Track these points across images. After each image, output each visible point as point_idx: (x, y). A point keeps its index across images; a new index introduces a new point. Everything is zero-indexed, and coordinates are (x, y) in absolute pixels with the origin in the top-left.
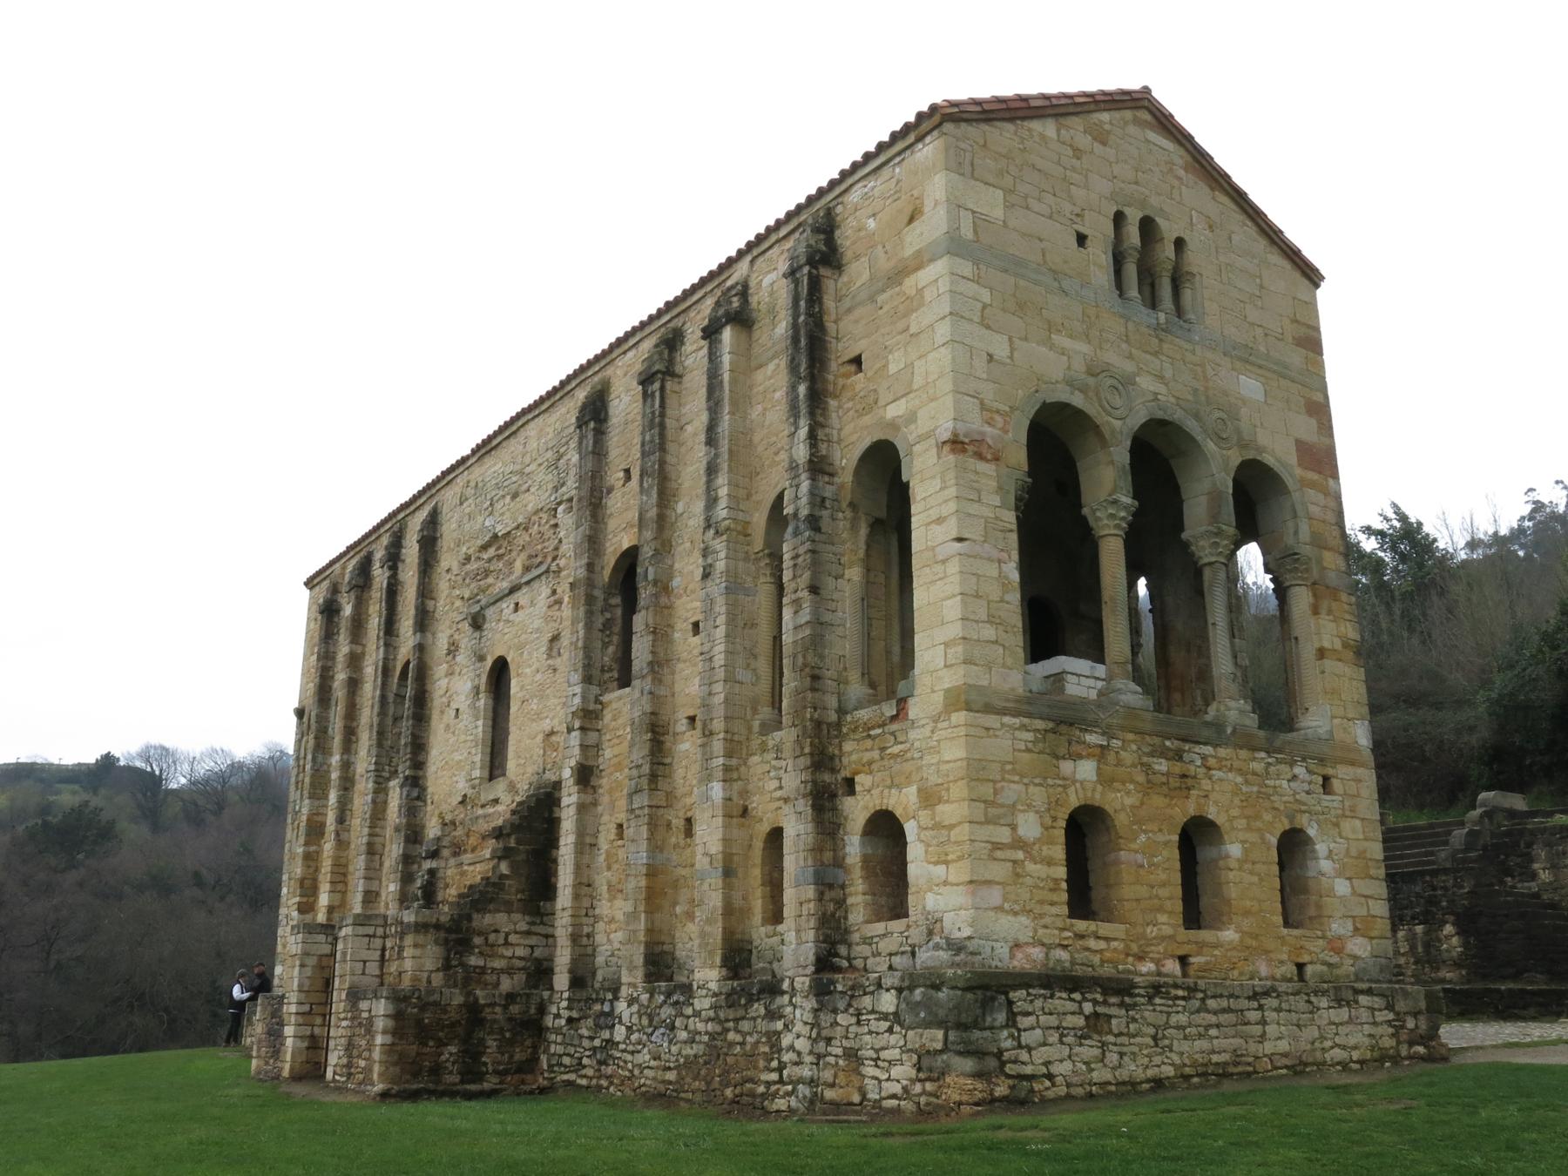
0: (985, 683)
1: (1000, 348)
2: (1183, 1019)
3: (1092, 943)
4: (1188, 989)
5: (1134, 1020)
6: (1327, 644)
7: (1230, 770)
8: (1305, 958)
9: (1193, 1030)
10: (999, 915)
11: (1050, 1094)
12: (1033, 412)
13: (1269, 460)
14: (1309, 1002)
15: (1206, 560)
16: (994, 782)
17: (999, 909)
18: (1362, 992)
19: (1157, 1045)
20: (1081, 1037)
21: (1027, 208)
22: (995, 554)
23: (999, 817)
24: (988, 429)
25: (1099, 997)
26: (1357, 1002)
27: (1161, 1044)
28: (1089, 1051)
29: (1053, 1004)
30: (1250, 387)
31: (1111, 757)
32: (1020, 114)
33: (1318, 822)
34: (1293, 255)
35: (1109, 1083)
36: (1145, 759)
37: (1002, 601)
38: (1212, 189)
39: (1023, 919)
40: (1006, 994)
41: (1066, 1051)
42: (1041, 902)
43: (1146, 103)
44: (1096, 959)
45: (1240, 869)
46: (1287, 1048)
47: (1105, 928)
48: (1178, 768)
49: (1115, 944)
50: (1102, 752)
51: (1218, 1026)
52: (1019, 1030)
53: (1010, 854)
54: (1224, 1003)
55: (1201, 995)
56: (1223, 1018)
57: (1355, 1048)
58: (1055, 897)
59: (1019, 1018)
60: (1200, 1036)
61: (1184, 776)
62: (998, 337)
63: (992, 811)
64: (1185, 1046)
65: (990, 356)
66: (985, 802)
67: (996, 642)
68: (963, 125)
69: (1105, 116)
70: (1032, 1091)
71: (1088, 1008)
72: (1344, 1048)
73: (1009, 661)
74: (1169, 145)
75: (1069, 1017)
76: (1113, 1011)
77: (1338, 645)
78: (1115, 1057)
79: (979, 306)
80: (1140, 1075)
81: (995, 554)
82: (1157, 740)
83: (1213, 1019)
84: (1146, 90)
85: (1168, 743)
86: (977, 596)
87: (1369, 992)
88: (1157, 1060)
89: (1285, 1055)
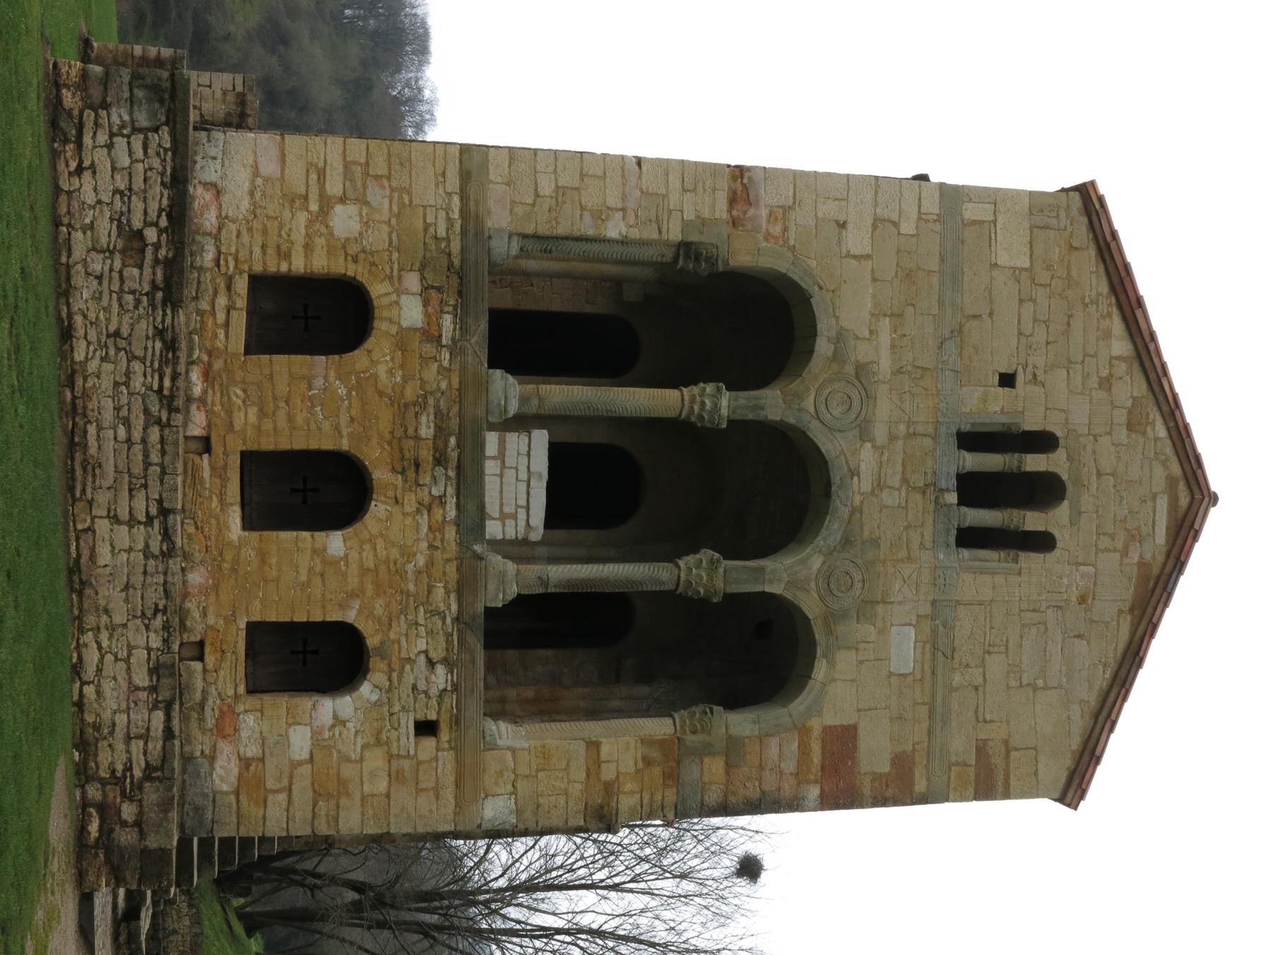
0: (492, 177)
1: (857, 240)
2: (137, 383)
3: (222, 301)
4: (172, 397)
5: (138, 303)
6: (605, 749)
7: (431, 547)
8: (210, 659)
9: (124, 400)
10: (249, 170)
11: (61, 166)
12: (796, 278)
13: (820, 670)
14: (156, 611)
16: (389, 178)
17: (256, 174)
18: (168, 718)
19: (108, 336)
20: (119, 221)
21: (1021, 301)
22: (631, 204)
23: (352, 181)
24: (764, 212)
25: (162, 252)
26: (156, 707)
27: (110, 342)
28: (106, 231)
29: (158, 189)
30: (904, 649)
31: (429, 349)
32: (1122, 297)
33: (378, 704)
35: (69, 256)
36: (431, 401)
37: (582, 208)
38: (1131, 610)
39: (245, 204)
40: (167, 124)
41: (106, 198)
42: (265, 232)
43: (1198, 496)
44: (204, 305)
45: (314, 551)
46: (101, 562)
47: (240, 321)
48: (426, 454)
49: (221, 334)
50: (430, 335)
51: (129, 440)
52: (128, 137)
53: (314, 190)
54: (155, 457)
55: (164, 418)
56: (138, 449)
59: (141, 136)
60: (117, 409)
61: (417, 465)
62: (867, 241)
63: (358, 170)
64: (106, 383)
65: (842, 225)
66: (367, 164)
67: (537, 195)
68: (1085, 220)
69: (1162, 432)
70: (66, 141)
71: (151, 235)
72: (99, 670)
73: (519, 210)
75: (141, 206)
76: (147, 270)
77: (608, 773)
78: (97, 267)
79: (895, 217)
80: (78, 305)
81: (631, 204)
82: (454, 423)
83: (137, 435)
84: (1214, 499)
85: (453, 441)
86: (583, 176)
87: (169, 734)
88: (92, 335)
89: (93, 557)
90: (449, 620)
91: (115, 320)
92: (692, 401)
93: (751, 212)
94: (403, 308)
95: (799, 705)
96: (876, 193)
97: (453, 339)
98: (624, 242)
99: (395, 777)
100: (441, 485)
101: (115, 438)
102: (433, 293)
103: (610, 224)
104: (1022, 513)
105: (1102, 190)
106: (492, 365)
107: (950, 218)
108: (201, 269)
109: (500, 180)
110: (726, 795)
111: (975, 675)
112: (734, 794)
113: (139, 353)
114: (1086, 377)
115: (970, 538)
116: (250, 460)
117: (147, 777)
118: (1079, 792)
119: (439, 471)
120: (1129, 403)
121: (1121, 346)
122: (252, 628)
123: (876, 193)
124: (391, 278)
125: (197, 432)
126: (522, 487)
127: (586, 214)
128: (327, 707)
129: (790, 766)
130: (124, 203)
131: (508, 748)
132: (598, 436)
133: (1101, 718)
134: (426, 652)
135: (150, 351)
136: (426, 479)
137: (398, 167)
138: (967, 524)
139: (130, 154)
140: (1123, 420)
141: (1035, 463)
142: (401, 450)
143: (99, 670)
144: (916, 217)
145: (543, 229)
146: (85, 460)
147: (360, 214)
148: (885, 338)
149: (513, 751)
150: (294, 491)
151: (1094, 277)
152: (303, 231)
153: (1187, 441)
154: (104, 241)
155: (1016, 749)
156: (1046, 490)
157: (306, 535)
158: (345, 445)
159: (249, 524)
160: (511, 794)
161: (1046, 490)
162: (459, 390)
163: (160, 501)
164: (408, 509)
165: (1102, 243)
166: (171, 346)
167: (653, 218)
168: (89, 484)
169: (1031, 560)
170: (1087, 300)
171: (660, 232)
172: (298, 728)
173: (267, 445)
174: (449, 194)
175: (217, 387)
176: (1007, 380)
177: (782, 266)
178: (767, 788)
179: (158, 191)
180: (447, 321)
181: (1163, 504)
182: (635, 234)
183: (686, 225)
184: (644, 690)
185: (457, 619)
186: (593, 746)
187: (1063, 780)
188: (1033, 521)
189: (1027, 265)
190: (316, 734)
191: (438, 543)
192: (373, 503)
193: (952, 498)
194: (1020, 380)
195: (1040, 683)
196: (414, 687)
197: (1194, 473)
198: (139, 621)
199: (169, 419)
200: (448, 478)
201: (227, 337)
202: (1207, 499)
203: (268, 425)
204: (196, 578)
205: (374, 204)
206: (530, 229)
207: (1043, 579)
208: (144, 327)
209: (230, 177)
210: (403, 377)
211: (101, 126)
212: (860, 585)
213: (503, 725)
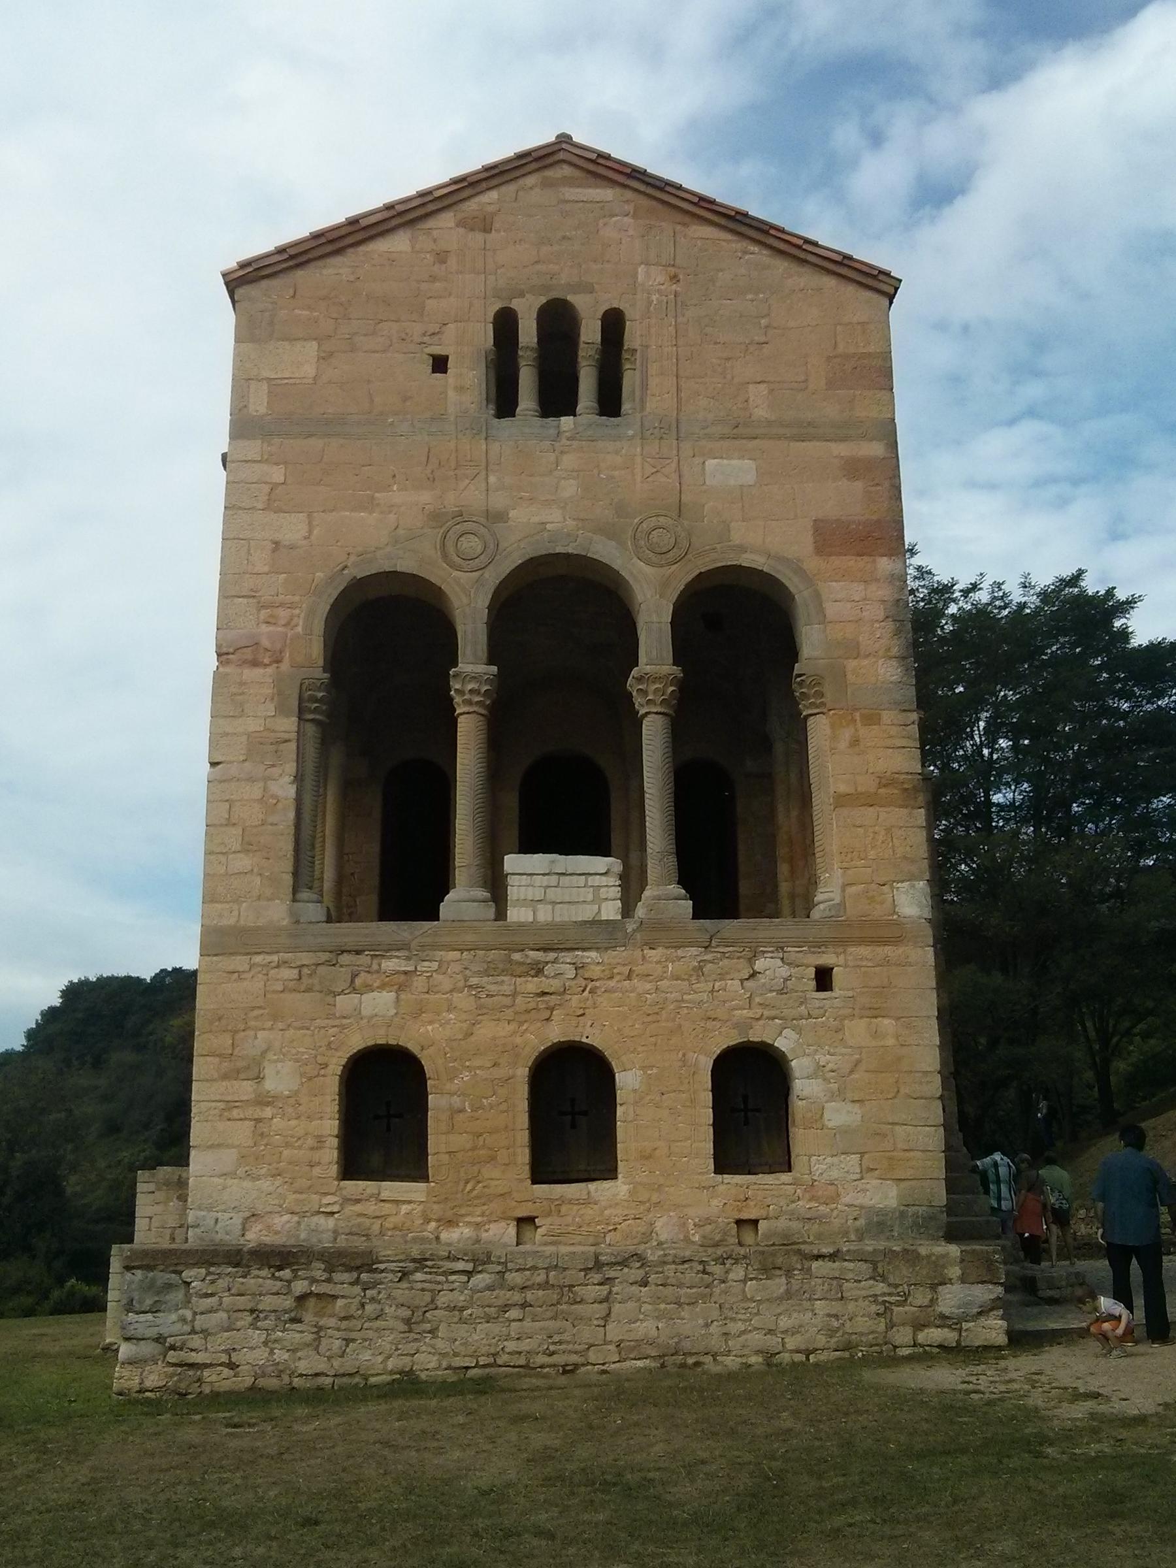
0: (232, 921)
1: (292, 529)
2: (460, 1298)
3: (371, 1208)
5: (373, 1299)
6: (843, 788)
7: (629, 978)
10: (230, 1182)
11: (225, 1386)
12: (335, 594)
14: (704, 1272)
15: (642, 712)
17: (232, 1174)
18: (818, 1257)
24: (264, 628)
28: (295, 1335)
29: (250, 1282)
30: (728, 471)
31: (419, 983)
33: (799, 1030)
34: (843, 268)
36: (474, 981)
39: (266, 1185)
40: (180, 1273)
43: (561, 156)
46: (654, 1333)
47: (390, 1189)
48: (532, 985)
49: (405, 1208)
50: (401, 983)
51: (524, 1305)
53: (251, 1112)
54: (540, 1278)
56: (529, 1296)
57: (794, 1331)
58: (316, 1156)
59: (194, 1299)
61: (544, 994)
64: (462, 1331)
65: (277, 543)
69: (494, 195)
71: (300, 1287)
72: (770, 1332)
74: (607, 194)
75: (268, 1299)
79: (267, 488)
83: (517, 1297)
84: (564, 139)
85: (517, 956)
86: (229, 823)
87: (833, 1257)
90: (708, 957)
91: (391, 1323)
92: (469, 702)
93: (265, 643)
94: (374, 1013)
95: (792, 582)
96: (240, 508)
97: (408, 958)
98: (299, 778)
99: (875, 1013)
100: (563, 967)
101: (520, 1320)
102: (358, 981)
103: (280, 793)
104: (582, 345)
105: (232, 264)
106: (434, 916)
107: (266, 427)
108: (336, 1233)
109: (236, 913)
110: (891, 658)
111: (757, 395)
112: (888, 650)
113: (427, 1297)
114: (433, 278)
115: (610, 402)
116: (540, 1175)
117: (884, 1278)
118: (881, 277)
119: (548, 969)
120: (461, 230)
121: (398, 243)
122: (720, 1169)
123: (240, 508)
124: (343, 1027)
125: (512, 1230)
126: (565, 880)
127: (270, 820)
128: (805, 1087)
129: (857, 590)
130: (266, 1318)
131: (843, 891)
132: (511, 801)
133: (802, 255)
134: (742, 981)
135: (426, 1285)
136: (555, 984)
137: (224, 1022)
138: (596, 405)
139: (211, 1311)
140: (479, 237)
141: (528, 333)
142: (528, 1011)
143: (770, 1332)
144: (265, 467)
145: (288, 865)
146: (544, 1353)
147: (276, 1061)
148: (397, 496)
149: (844, 887)
150: (573, 1126)
151: (325, 272)
152: (293, 1123)
153: (502, 168)
154: (309, 1337)
155: (835, 346)
156: (558, 320)
157: (620, 1111)
158: (523, 1072)
159: (611, 1173)
160: (892, 888)
161: (558, 320)
162: (462, 951)
163: (587, 1270)
164: (589, 1003)
165: (291, 263)
166: (420, 1262)
167: (273, 747)
168: (570, 1347)
169: (633, 336)
170: (352, 278)
171: (289, 741)
172: (826, 1116)
173: (523, 1156)
174: (251, 966)
175: (463, 1211)
176: (440, 364)
177: (324, 608)
178: (882, 616)
179: (253, 1281)
180: (389, 965)
181: (571, 193)
182: (291, 767)
183: (281, 710)
184: (779, 748)
185: (706, 948)
186: (842, 801)
187: (869, 294)
188: (590, 333)
189: (314, 344)
190: (832, 1099)
191: (626, 970)
192: (584, 1040)
193: (566, 422)
194: (438, 350)
195: (763, 322)
196: (781, 992)
197: (537, 160)
198: (717, 1291)
199: (499, 1263)
200: (555, 961)
201: (410, 1202)
202: (564, 146)
203: (503, 1156)
204: (665, 1227)
205: (264, 1046)
206: (288, 879)
207: (653, 321)
208: (401, 1292)
209: (237, 1204)
210: (448, 1011)
211: (184, 1344)
212: (661, 519)
213: (819, 897)
